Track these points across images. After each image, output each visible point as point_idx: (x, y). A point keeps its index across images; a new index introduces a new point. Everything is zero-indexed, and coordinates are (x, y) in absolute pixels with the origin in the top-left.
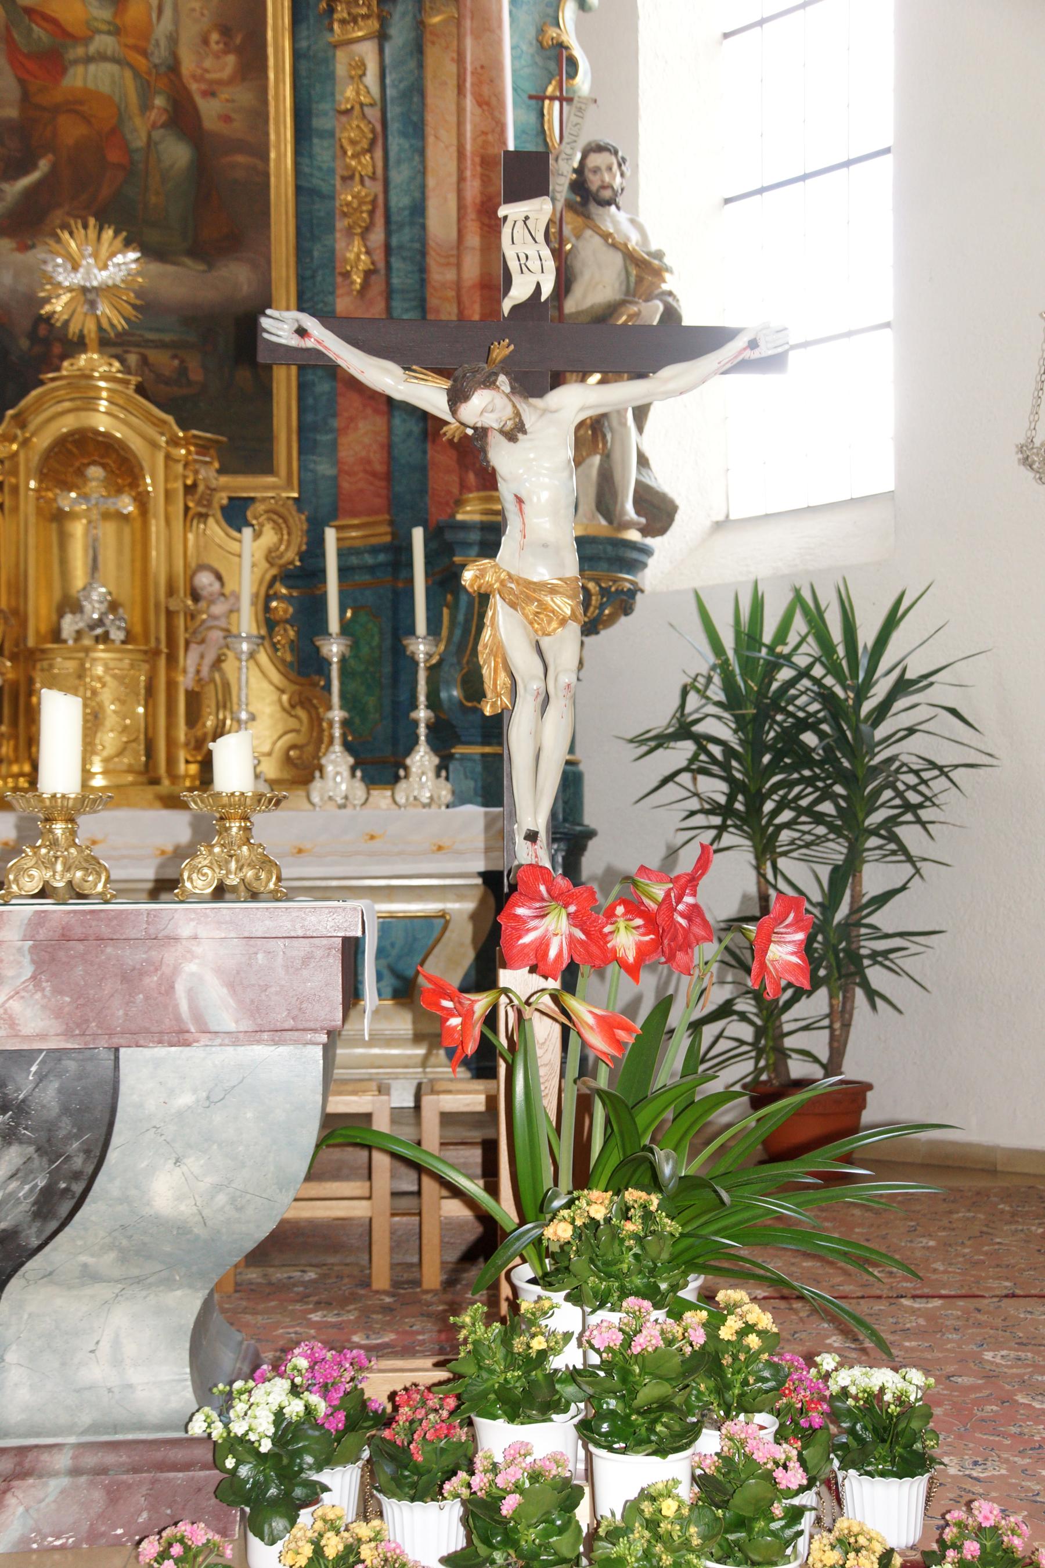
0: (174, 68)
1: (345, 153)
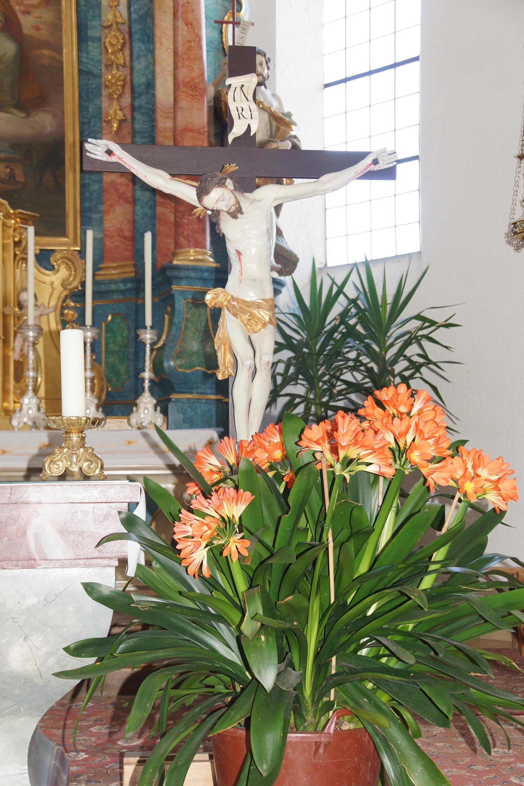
1: (107, 51)
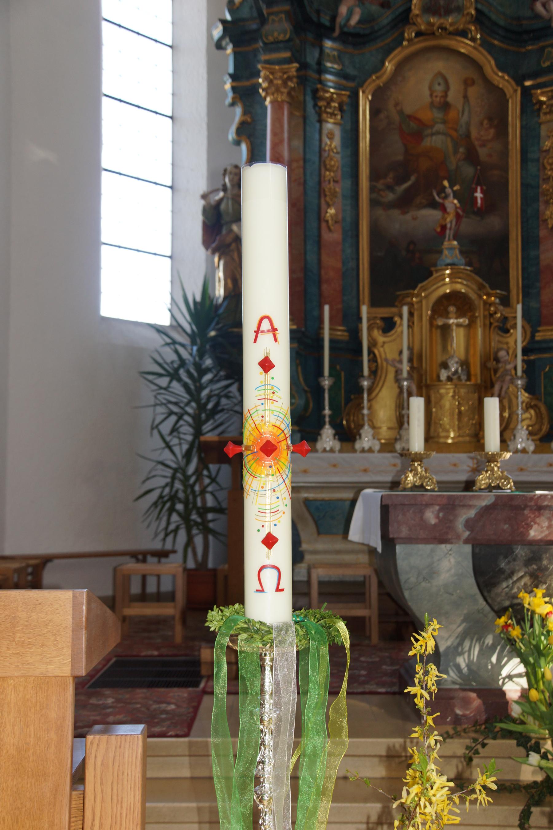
0: (468, 135)
